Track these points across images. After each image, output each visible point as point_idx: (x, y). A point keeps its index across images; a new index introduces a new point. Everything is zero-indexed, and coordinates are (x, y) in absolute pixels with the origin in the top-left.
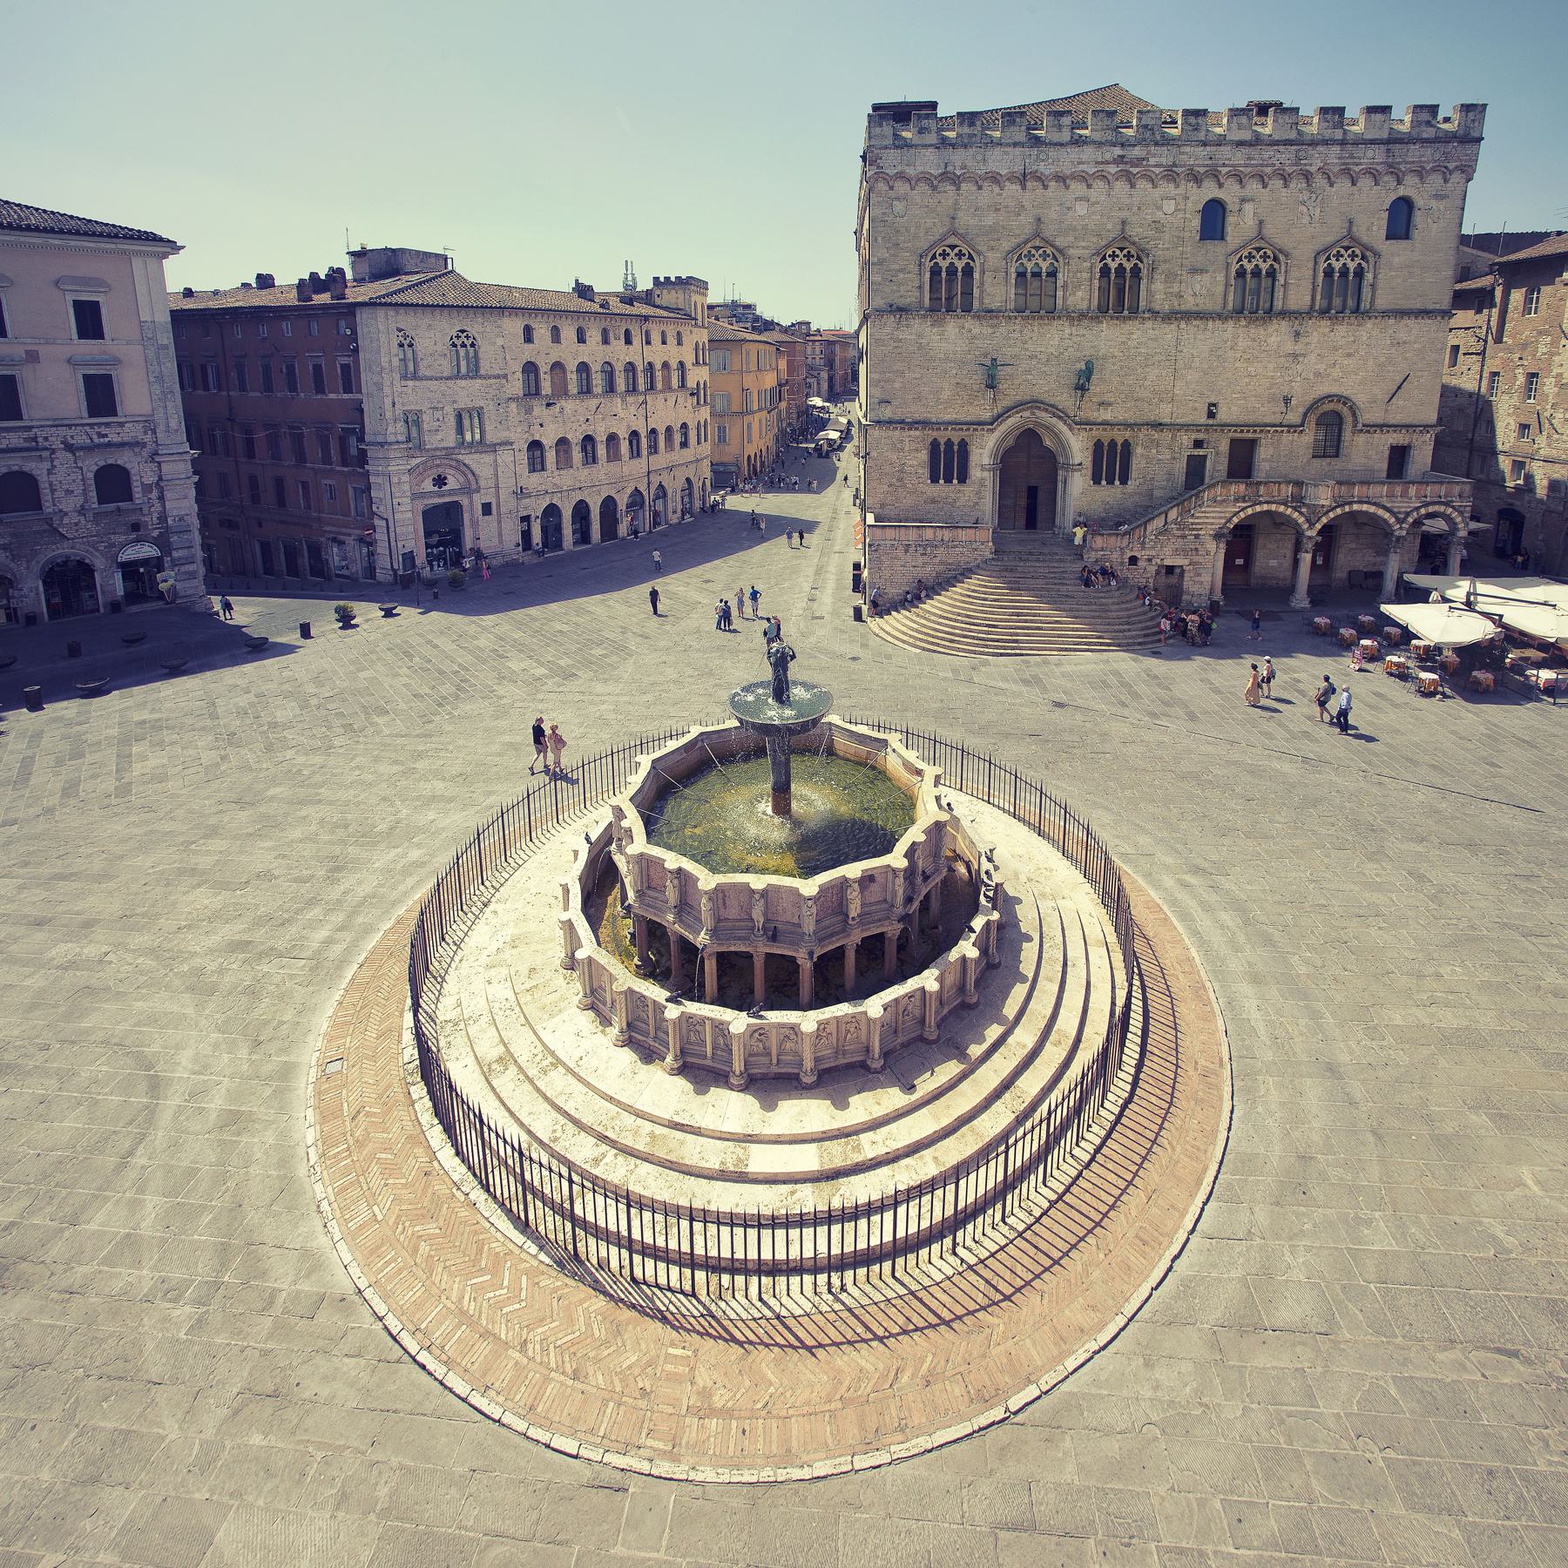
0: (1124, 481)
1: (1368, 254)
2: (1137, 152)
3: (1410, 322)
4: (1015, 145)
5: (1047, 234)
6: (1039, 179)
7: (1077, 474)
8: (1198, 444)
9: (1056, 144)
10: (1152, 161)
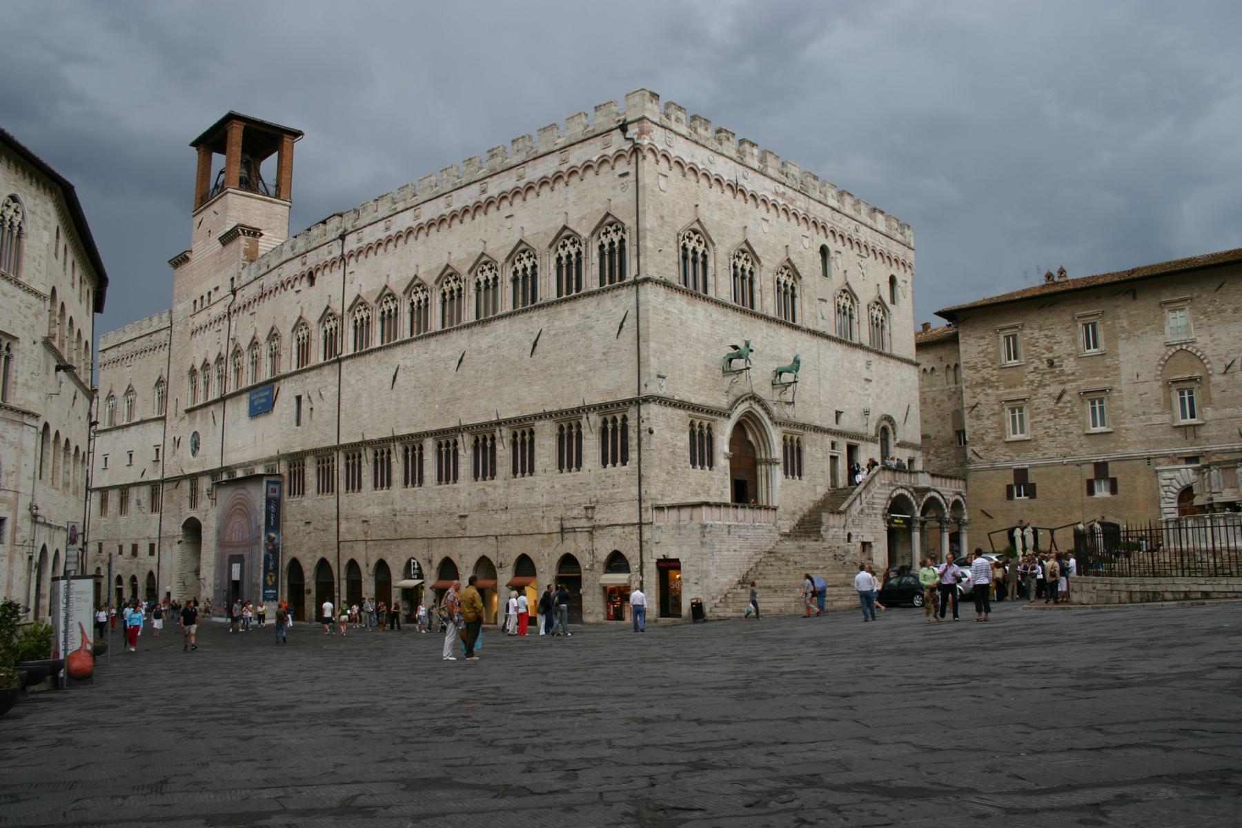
0: (800, 475)
1: (886, 311)
2: (790, 193)
3: (905, 365)
4: (731, 159)
5: (749, 241)
6: (742, 191)
7: (777, 467)
8: (833, 445)
9: (752, 169)
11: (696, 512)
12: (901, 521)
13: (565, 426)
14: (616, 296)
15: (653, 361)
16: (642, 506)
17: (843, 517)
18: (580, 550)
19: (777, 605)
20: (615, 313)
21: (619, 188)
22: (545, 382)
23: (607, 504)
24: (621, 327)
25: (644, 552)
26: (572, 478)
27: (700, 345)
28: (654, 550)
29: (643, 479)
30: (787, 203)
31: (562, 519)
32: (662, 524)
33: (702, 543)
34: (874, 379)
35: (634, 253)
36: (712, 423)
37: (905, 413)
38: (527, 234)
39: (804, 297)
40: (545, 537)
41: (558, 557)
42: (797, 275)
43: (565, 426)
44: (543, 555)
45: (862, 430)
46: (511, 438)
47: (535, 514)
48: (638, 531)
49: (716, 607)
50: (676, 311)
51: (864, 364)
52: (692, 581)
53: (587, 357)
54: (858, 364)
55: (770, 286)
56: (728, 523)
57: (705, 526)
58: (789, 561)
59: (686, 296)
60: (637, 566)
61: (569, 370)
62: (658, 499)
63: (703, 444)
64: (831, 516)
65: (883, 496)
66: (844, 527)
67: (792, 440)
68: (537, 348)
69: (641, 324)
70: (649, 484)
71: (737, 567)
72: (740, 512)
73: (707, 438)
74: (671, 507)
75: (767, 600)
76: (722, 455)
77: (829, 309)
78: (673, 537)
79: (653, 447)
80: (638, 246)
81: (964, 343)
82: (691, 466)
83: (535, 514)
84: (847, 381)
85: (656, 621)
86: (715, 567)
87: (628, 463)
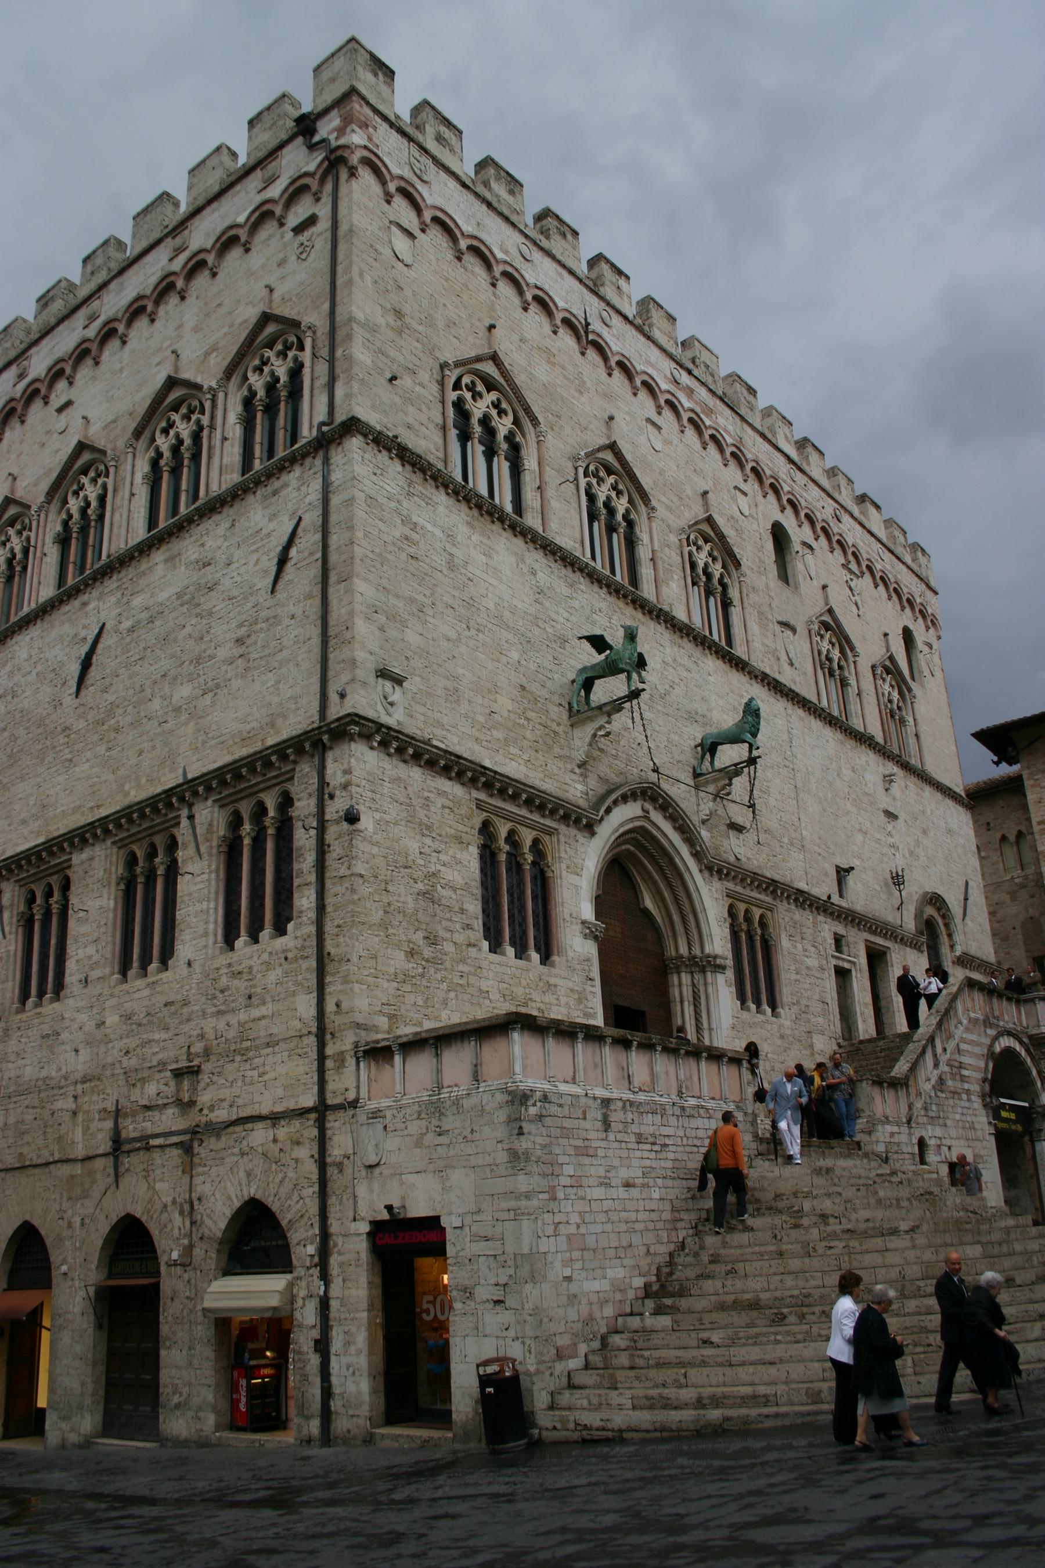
0: (773, 1005)
2: (703, 393)
7: (721, 978)
8: (838, 941)
10: (721, 421)
11: (492, 1052)
12: (1013, 1116)
13: (140, 854)
14: (275, 493)
15: (361, 626)
16: (329, 1051)
17: (902, 1093)
18: (159, 1206)
19: (796, 1370)
20: (269, 535)
21: (294, 258)
22: (102, 749)
23: (231, 1055)
24: (283, 560)
25: (332, 1200)
26: (146, 992)
27: (505, 634)
28: (362, 1191)
29: (330, 968)
30: (698, 410)
31: (118, 1113)
32: (385, 1103)
33: (514, 1156)
34: (902, 816)
35: (323, 380)
36: (546, 838)
37: (962, 897)
38: (94, 429)
39: (748, 610)
40: (78, 1169)
41: (104, 1227)
42: (731, 559)
43: (140, 854)
44: (70, 1225)
45: (891, 917)
46: (22, 908)
47: (60, 1104)
48: (315, 1132)
49: (571, 1386)
50: (438, 532)
51: (879, 779)
52: (484, 1293)
53: (198, 660)
54: (869, 777)
55: (672, 557)
56: (601, 1093)
57: (520, 1098)
58: (799, 1213)
59: (463, 506)
60: (311, 1249)
61: (156, 704)
62: (376, 1029)
63: (522, 893)
64: (876, 1092)
65: (978, 1050)
66: (909, 1122)
67: (748, 918)
68: (93, 673)
69: (334, 540)
70: (346, 980)
71: (636, 1240)
72: (638, 1063)
73: (534, 878)
74: (413, 1045)
75: (755, 1353)
76: (578, 927)
77: (800, 647)
78: (419, 1144)
79: (360, 868)
80: (332, 361)
81: (1033, 786)
82: (485, 945)
83: (60, 1104)
84: (849, 807)
85: (369, 1440)
86: (562, 1243)
87: (290, 927)
